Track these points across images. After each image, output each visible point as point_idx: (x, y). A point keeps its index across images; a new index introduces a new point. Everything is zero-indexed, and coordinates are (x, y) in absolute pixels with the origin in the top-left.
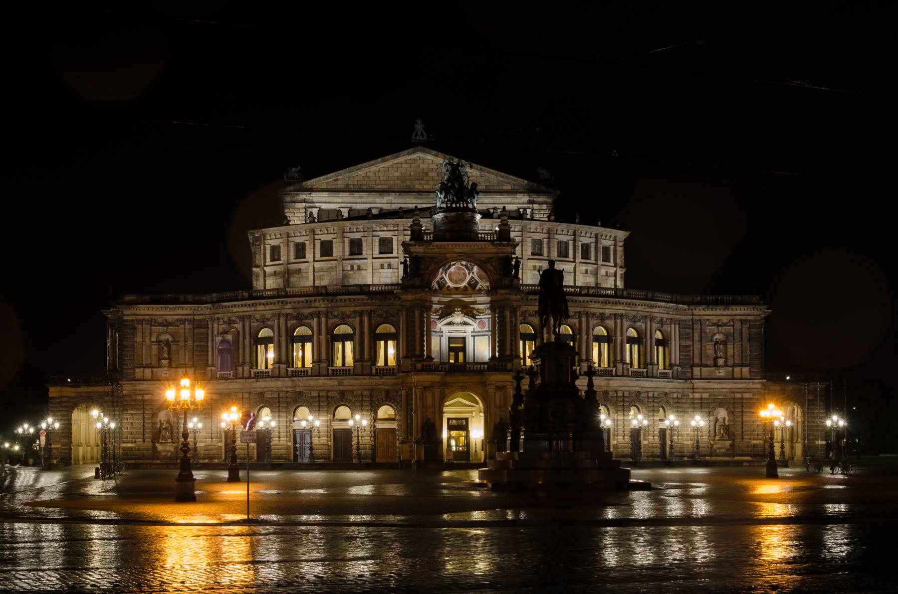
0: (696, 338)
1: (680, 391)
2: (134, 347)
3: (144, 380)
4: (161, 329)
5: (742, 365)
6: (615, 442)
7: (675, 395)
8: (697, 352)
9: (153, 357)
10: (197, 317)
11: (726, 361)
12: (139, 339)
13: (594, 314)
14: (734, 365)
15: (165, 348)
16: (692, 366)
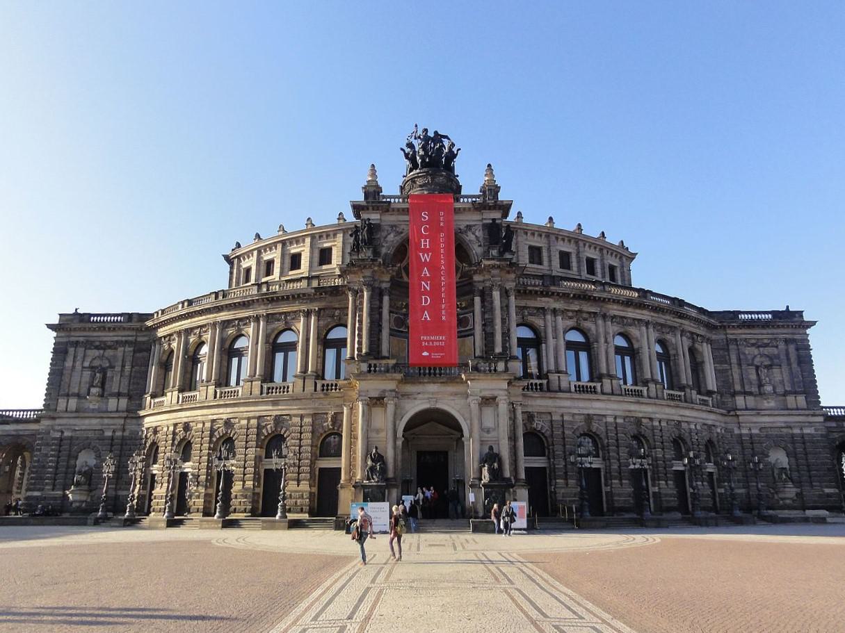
0: (734, 360)
1: (723, 425)
2: (62, 374)
4: (96, 353)
5: (796, 393)
6: (656, 489)
7: (719, 430)
8: (736, 377)
9: (82, 385)
10: (140, 339)
11: (774, 388)
12: (69, 364)
13: (614, 317)
14: (786, 394)
15: (98, 375)
16: (734, 394)
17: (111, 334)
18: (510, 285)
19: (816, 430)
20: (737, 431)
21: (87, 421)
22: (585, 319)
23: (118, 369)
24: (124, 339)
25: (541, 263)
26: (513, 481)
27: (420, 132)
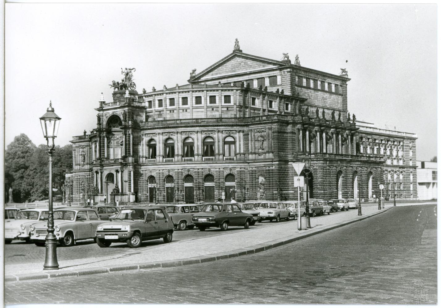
1: (242, 167)
3: (77, 170)
5: (268, 152)
7: (239, 169)
8: (250, 146)
12: (76, 154)
16: (249, 154)
17: (84, 143)
18: (130, 132)
19: (275, 167)
20: (249, 169)
21: (82, 173)
22: (172, 135)
23: (87, 155)
24: (87, 144)
25: (187, 104)
26: (128, 193)
27: (124, 70)
